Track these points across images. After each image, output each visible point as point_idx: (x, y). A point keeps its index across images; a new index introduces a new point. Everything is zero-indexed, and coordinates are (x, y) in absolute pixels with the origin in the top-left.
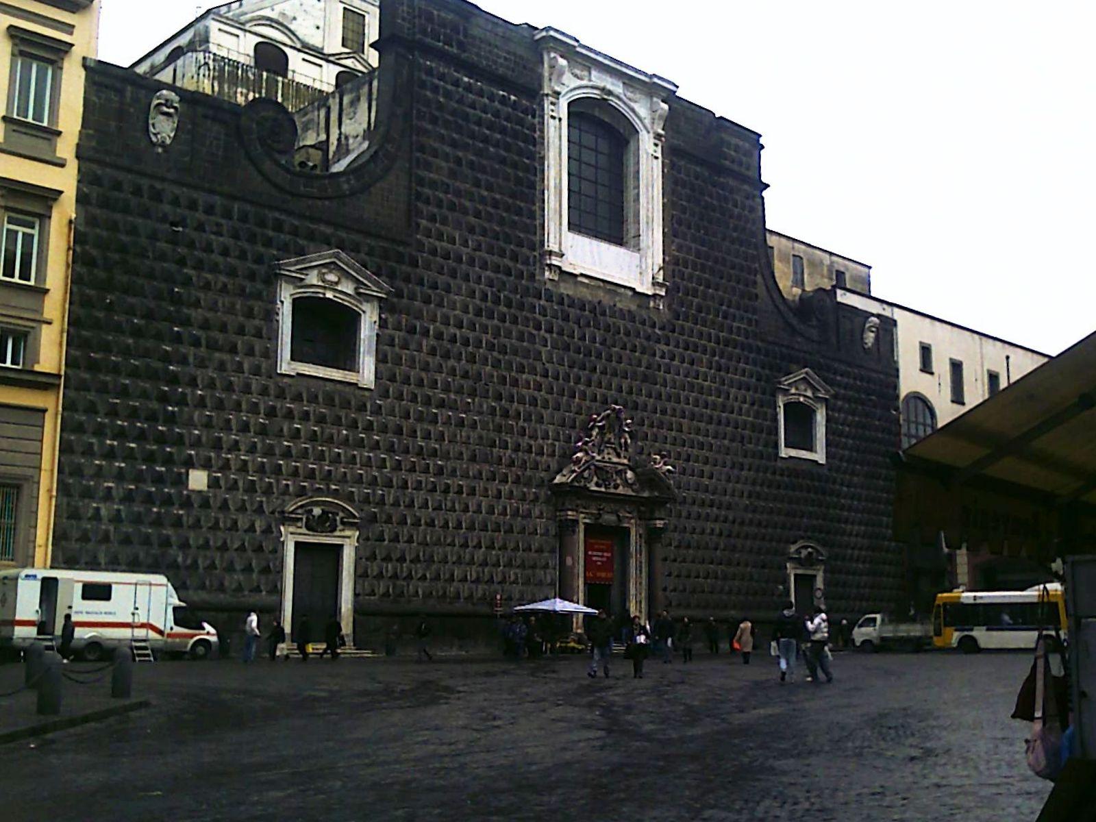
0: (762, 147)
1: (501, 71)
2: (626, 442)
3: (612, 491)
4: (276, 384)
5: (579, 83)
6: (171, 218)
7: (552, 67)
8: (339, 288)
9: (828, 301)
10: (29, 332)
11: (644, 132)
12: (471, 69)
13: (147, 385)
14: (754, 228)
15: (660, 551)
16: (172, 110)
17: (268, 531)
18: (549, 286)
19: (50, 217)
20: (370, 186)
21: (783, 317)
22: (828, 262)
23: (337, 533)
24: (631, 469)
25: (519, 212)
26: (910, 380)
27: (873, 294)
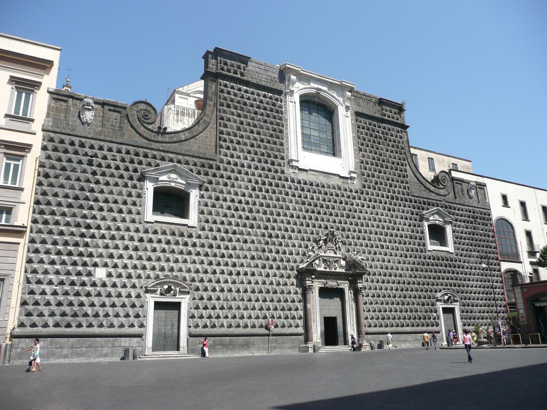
1: (264, 84)
2: (339, 247)
3: (333, 270)
4: (144, 227)
5: (303, 86)
6: (90, 154)
7: (289, 80)
9: (447, 176)
10: (13, 208)
11: (340, 106)
12: (248, 84)
13: (74, 230)
14: (403, 146)
15: (362, 299)
16: (90, 107)
17: (138, 296)
18: (293, 176)
19: (26, 156)
20: (196, 136)
21: (423, 185)
22: (448, 160)
23: (177, 296)
24: (344, 259)
25: (275, 143)
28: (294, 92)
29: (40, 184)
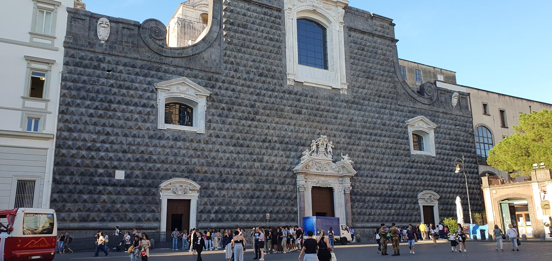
0: (394, 25)
3: (325, 171)
8: (187, 93)
16: (106, 26)
26: (478, 118)
27: (457, 84)
28: (292, 10)
29: (63, 96)
